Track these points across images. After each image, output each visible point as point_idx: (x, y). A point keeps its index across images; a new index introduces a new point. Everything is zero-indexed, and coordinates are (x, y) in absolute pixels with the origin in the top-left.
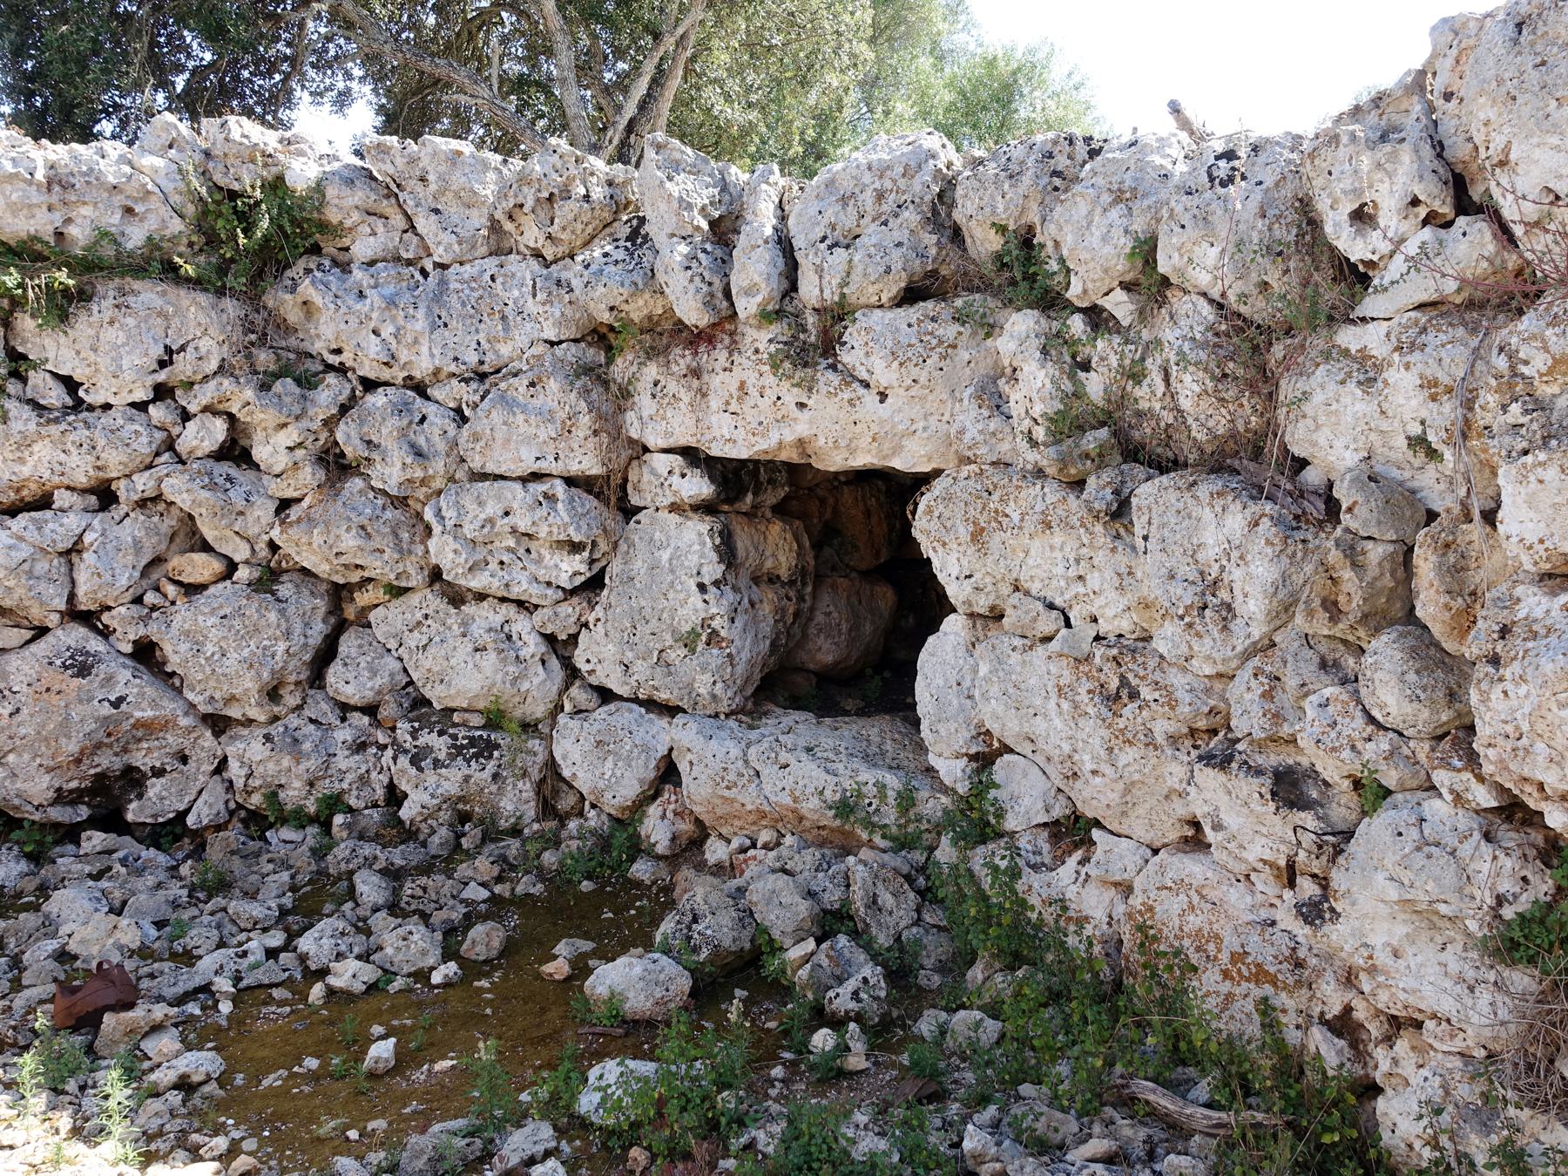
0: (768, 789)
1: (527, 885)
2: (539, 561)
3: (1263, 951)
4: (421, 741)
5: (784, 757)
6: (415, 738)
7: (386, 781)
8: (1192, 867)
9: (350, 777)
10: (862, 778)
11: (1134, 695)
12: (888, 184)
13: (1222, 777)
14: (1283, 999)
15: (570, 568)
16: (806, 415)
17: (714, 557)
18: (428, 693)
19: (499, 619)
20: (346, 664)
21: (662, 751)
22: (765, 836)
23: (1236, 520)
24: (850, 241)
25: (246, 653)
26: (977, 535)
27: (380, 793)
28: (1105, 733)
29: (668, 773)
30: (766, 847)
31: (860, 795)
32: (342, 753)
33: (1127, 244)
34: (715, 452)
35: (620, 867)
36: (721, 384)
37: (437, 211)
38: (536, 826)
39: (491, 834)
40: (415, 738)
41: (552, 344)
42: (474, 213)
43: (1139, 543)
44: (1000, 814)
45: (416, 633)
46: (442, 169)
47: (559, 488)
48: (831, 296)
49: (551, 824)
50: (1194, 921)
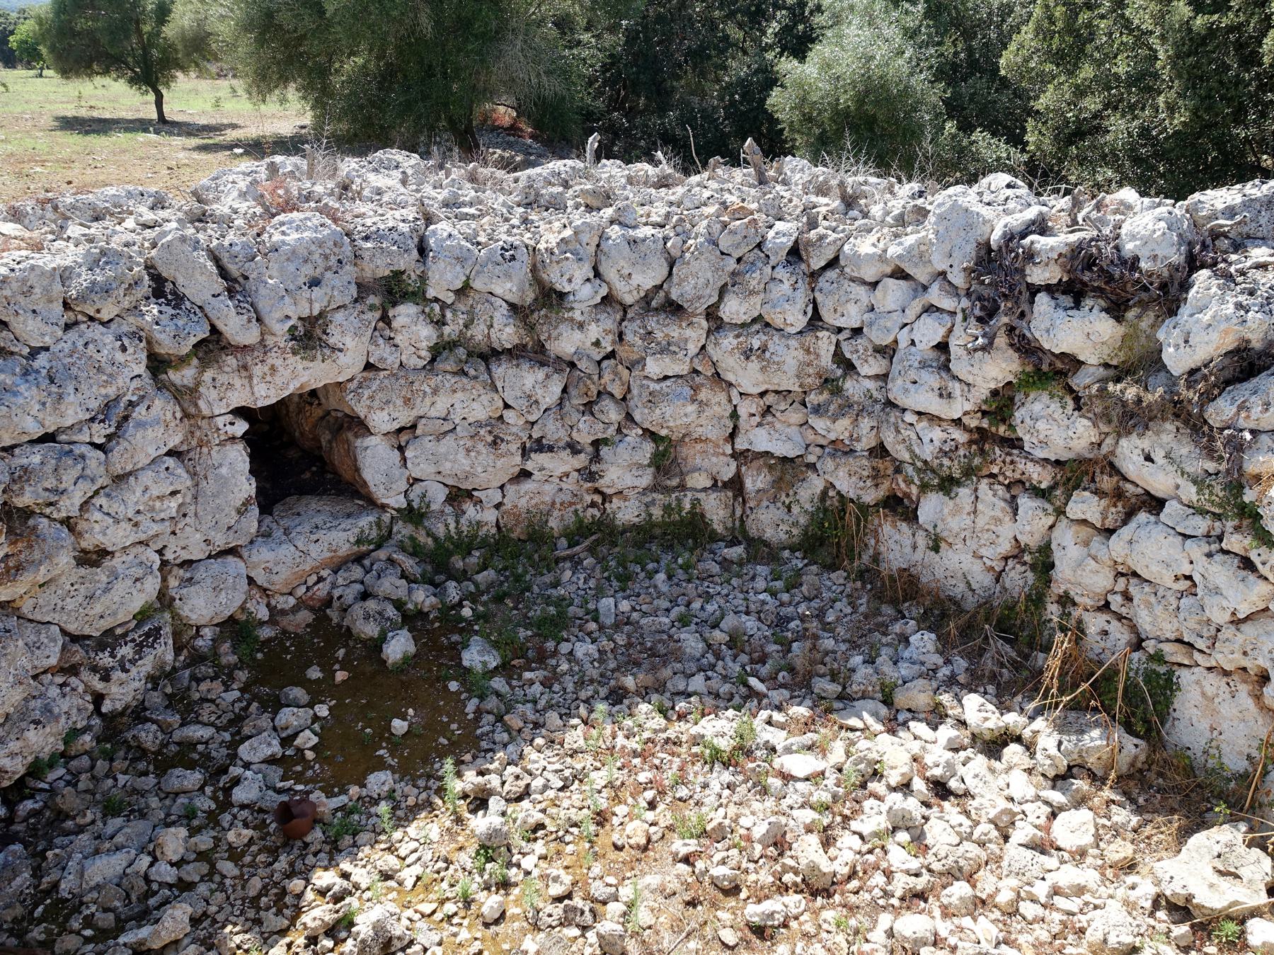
0: (314, 555)
1: (242, 676)
2: (152, 509)
3: (567, 498)
4: (119, 656)
5: (314, 537)
6: (114, 657)
7: (89, 698)
8: (528, 486)
9: (75, 711)
10: (361, 524)
11: (502, 440)
12: (328, 251)
13: (549, 454)
14: (579, 507)
15: (174, 504)
16: (308, 372)
17: (248, 459)
18: (87, 631)
19: (131, 557)
20: (38, 648)
21: (244, 572)
22: (314, 578)
23: (540, 374)
24: (315, 283)
25: (11, 679)
26: (407, 401)
27: (91, 707)
28: (492, 457)
29: (251, 581)
30: (315, 584)
31: (362, 531)
32: (60, 701)
33: (464, 278)
34: (260, 404)
35: (256, 639)
36: (258, 370)
37: (34, 311)
38: (182, 658)
39: (171, 675)
40: (114, 657)
41: (139, 376)
42: (55, 304)
43: (500, 389)
44: (428, 506)
45: (68, 600)
46: (45, 283)
47: (170, 462)
48: (316, 313)
49: (185, 651)
50: (533, 502)
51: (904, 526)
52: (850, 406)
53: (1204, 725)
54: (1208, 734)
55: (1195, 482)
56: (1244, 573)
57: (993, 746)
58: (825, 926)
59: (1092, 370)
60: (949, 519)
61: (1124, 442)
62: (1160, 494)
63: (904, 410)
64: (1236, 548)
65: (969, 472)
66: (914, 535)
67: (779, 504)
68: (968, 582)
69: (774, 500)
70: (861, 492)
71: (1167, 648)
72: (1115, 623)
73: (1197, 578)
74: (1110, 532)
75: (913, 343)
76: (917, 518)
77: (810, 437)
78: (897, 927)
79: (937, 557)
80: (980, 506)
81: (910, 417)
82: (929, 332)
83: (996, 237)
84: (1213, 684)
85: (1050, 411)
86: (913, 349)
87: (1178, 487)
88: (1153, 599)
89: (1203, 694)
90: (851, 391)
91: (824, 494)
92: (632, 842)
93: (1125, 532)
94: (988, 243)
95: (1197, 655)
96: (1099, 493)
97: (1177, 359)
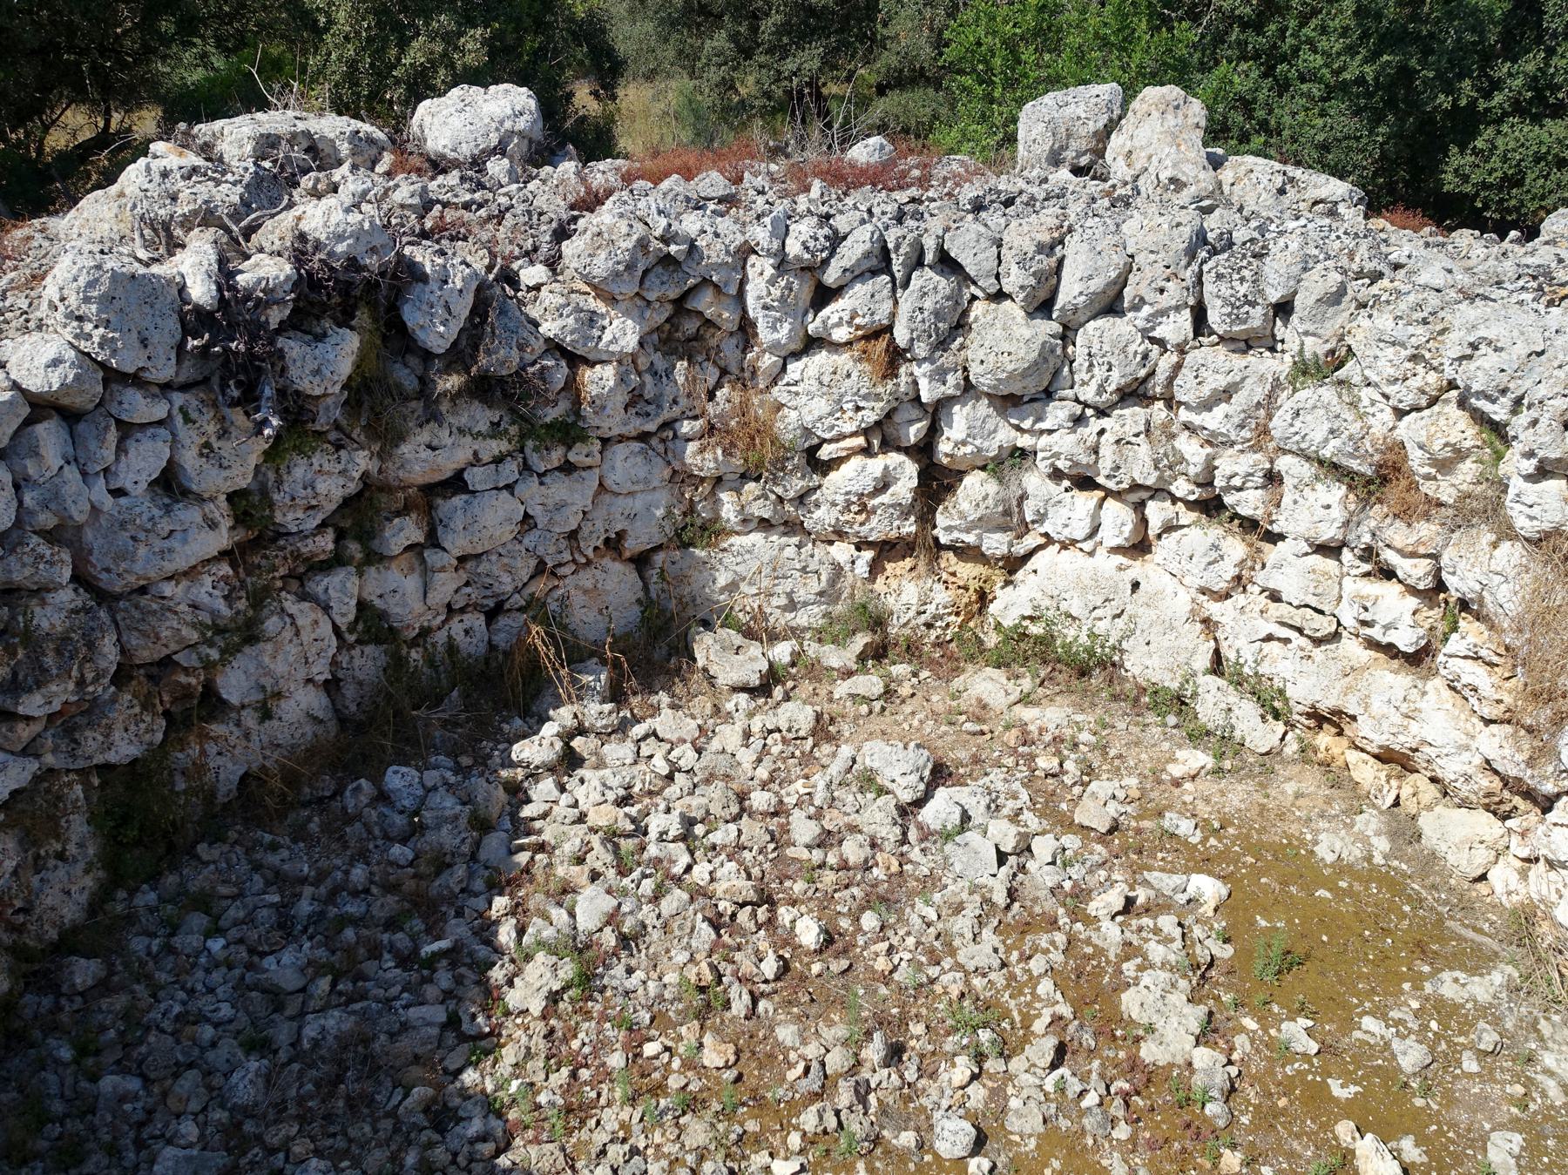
51: (217, 729)
52: (65, 639)
53: (591, 616)
54: (600, 618)
55: (492, 437)
56: (576, 475)
57: (569, 761)
58: (810, 893)
59: (330, 401)
60: (272, 666)
61: (405, 449)
62: (449, 474)
63: (143, 590)
64: (556, 464)
65: (259, 599)
66: (238, 724)
67: (52, 862)
68: (315, 718)
69: (38, 865)
70: (147, 737)
71: (531, 589)
72: (465, 617)
73: (536, 511)
74: (433, 541)
75: (118, 493)
76: (224, 702)
77: (24, 732)
78: (807, 839)
79: (275, 723)
80: (300, 622)
81: (168, 589)
82: (145, 460)
83: (201, 291)
84: (586, 579)
85: (316, 467)
86: (123, 501)
87: (475, 454)
88: (506, 560)
89: (586, 592)
90: (45, 624)
91: (87, 787)
92: (732, 1059)
93: (458, 522)
94: (198, 309)
95: (561, 571)
96: (398, 514)
97: (438, 333)
